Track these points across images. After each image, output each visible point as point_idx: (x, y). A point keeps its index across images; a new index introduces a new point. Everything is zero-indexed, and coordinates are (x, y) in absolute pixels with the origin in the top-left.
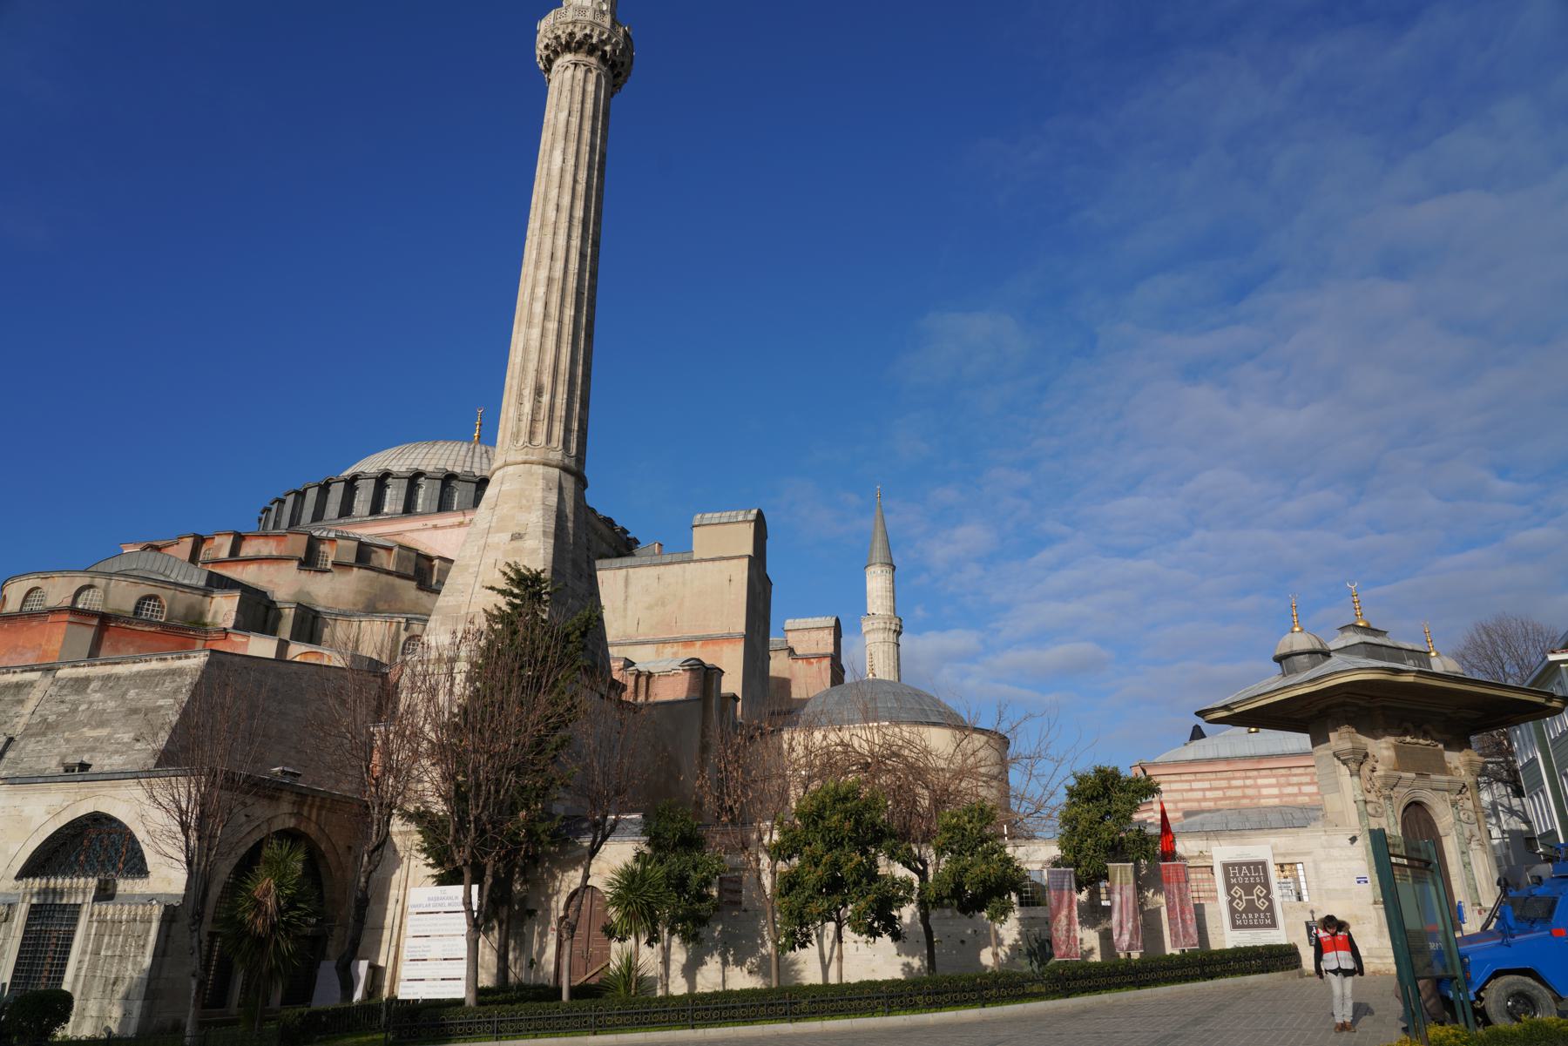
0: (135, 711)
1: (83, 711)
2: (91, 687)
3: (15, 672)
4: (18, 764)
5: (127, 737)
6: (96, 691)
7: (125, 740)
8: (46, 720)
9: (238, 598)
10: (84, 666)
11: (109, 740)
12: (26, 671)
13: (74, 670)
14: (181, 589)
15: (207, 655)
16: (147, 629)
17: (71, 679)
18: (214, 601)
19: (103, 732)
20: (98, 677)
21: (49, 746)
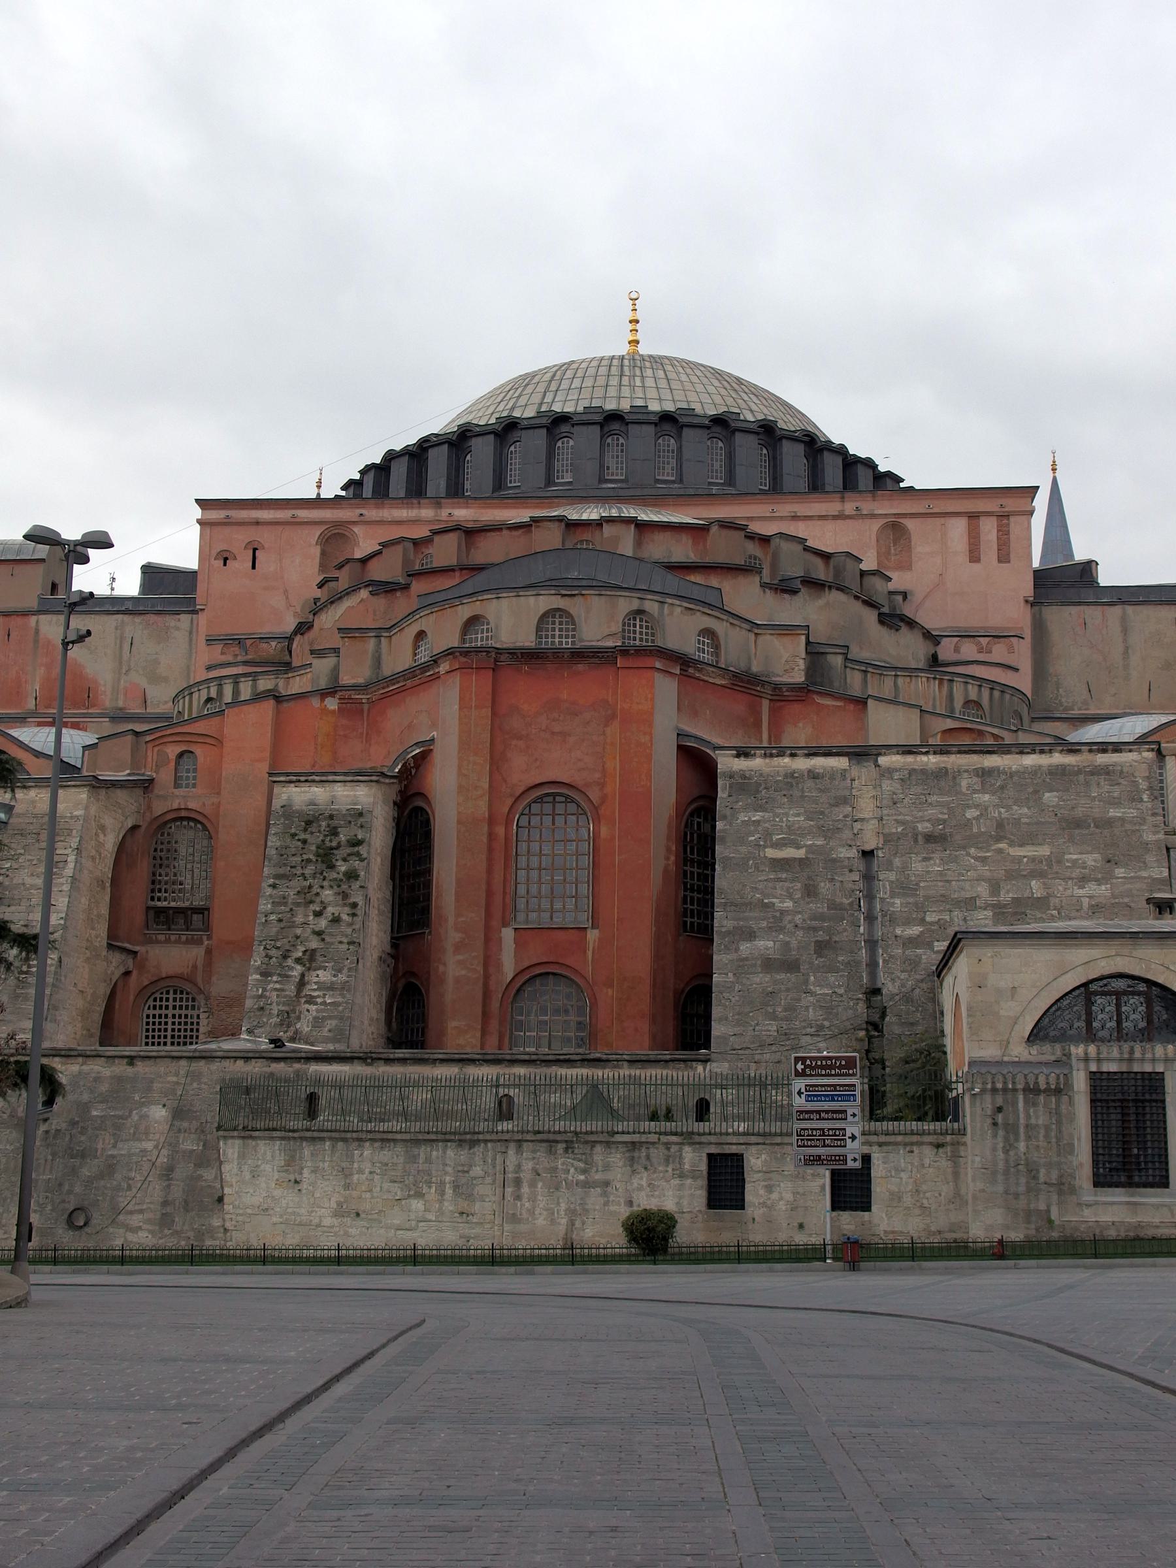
0: (1078, 824)
1: (977, 818)
2: (964, 783)
3: (793, 755)
4: (916, 890)
5: (1092, 859)
6: (975, 791)
7: (1090, 863)
8: (915, 828)
9: (803, 638)
10: (927, 753)
11: (1059, 862)
12: (815, 754)
13: (910, 759)
14: (731, 620)
15: (1153, 750)
16: (719, 682)
17: (912, 772)
18: (761, 639)
19: (1044, 851)
20: (966, 771)
21: (953, 866)
